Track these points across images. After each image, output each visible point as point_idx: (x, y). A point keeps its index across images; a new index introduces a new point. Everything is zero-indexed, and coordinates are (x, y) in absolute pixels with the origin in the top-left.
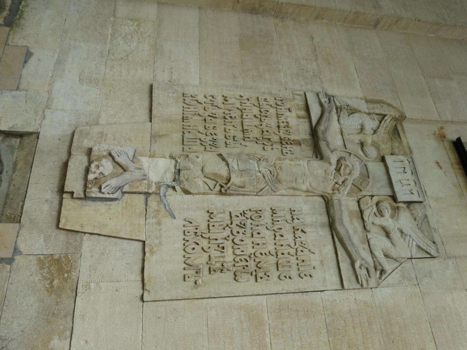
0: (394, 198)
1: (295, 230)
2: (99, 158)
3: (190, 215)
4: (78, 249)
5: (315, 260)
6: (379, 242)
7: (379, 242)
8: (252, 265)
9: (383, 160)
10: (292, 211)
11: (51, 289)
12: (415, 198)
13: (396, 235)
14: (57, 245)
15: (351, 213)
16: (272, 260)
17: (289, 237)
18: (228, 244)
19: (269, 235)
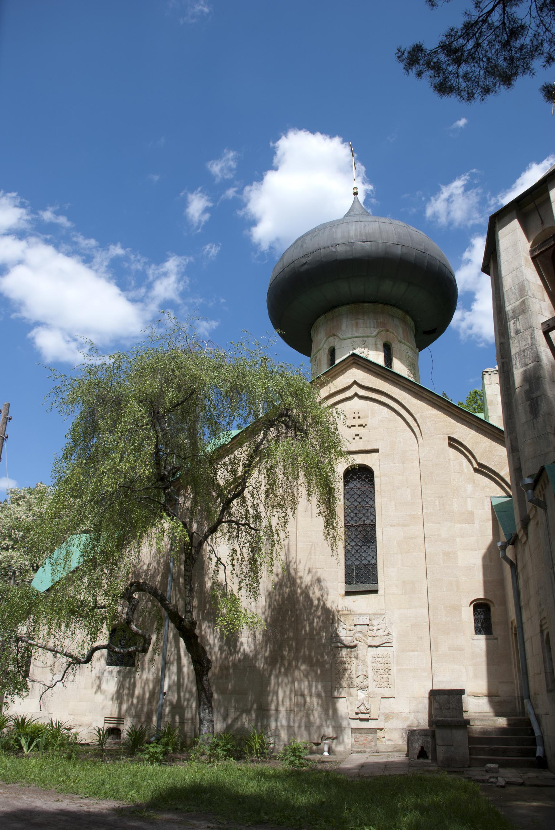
0: (368, 625)
1: (378, 657)
2: (360, 710)
3: (374, 686)
4: (383, 714)
5: (386, 653)
6: (381, 633)
7: (381, 633)
8: (387, 670)
9: (355, 625)
10: (373, 658)
11: (392, 719)
12: (368, 618)
13: (379, 627)
14: (381, 718)
15: (373, 640)
16: (386, 665)
17: (380, 659)
18: (382, 676)
19: (379, 665)
